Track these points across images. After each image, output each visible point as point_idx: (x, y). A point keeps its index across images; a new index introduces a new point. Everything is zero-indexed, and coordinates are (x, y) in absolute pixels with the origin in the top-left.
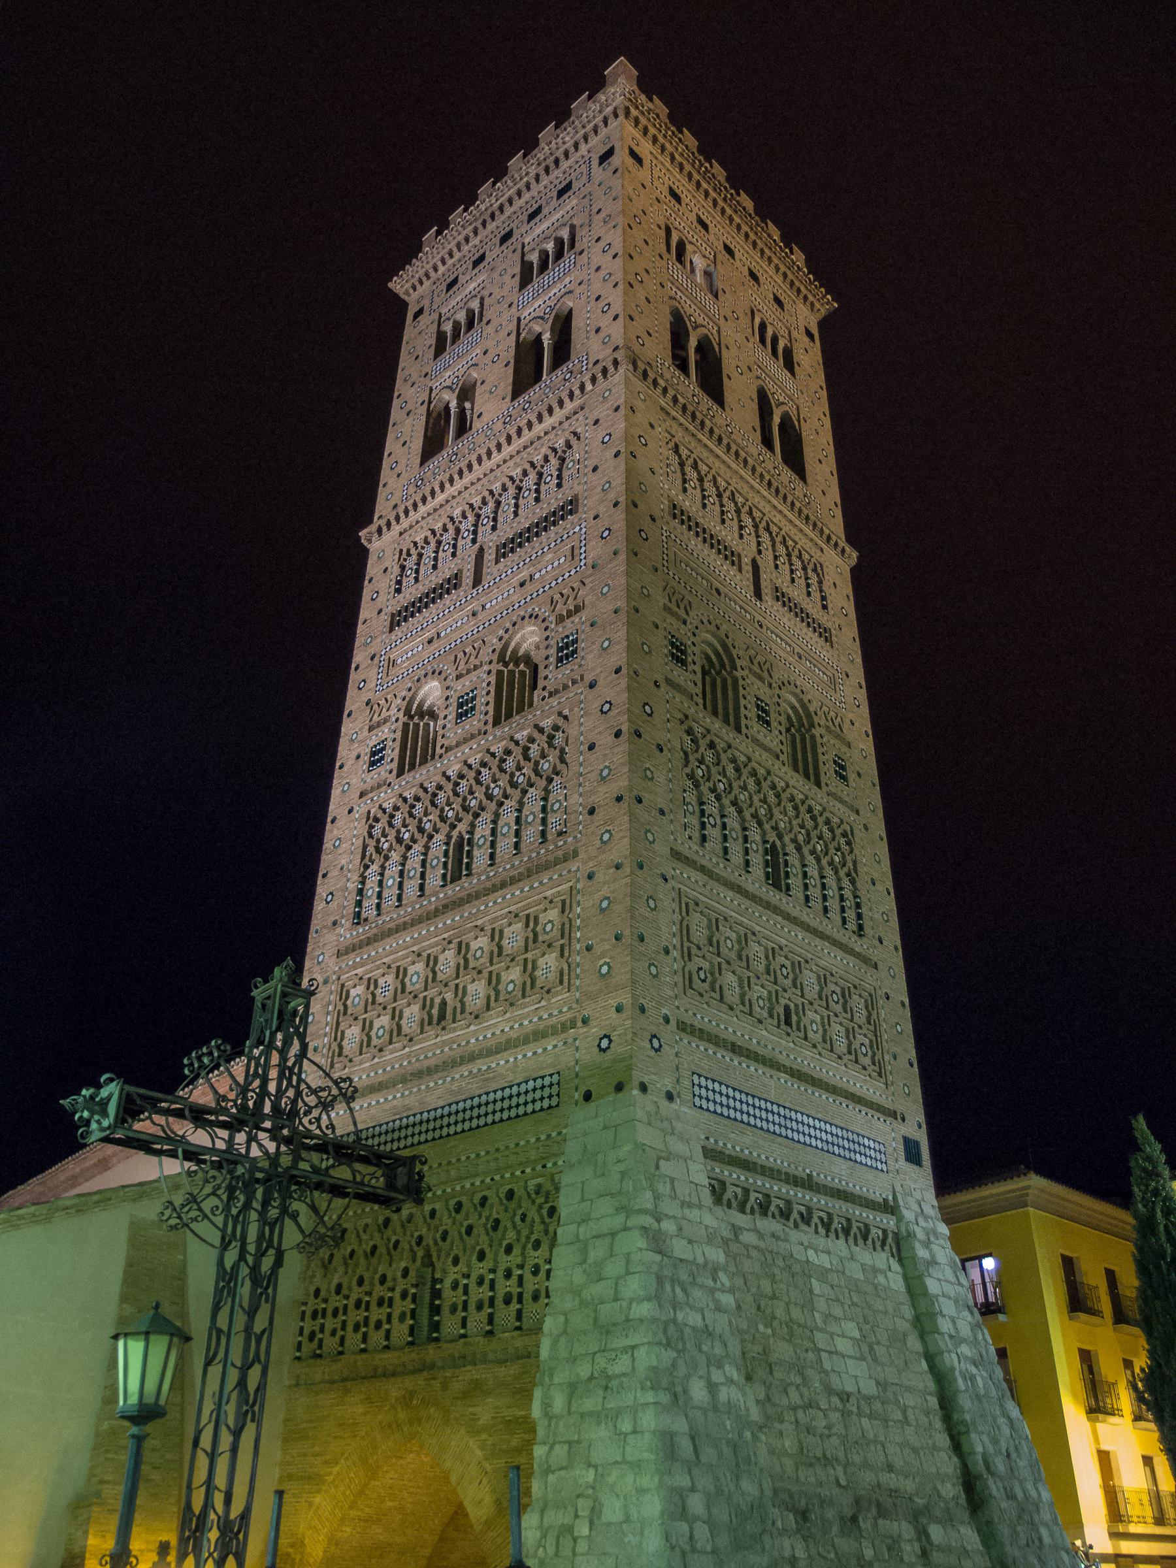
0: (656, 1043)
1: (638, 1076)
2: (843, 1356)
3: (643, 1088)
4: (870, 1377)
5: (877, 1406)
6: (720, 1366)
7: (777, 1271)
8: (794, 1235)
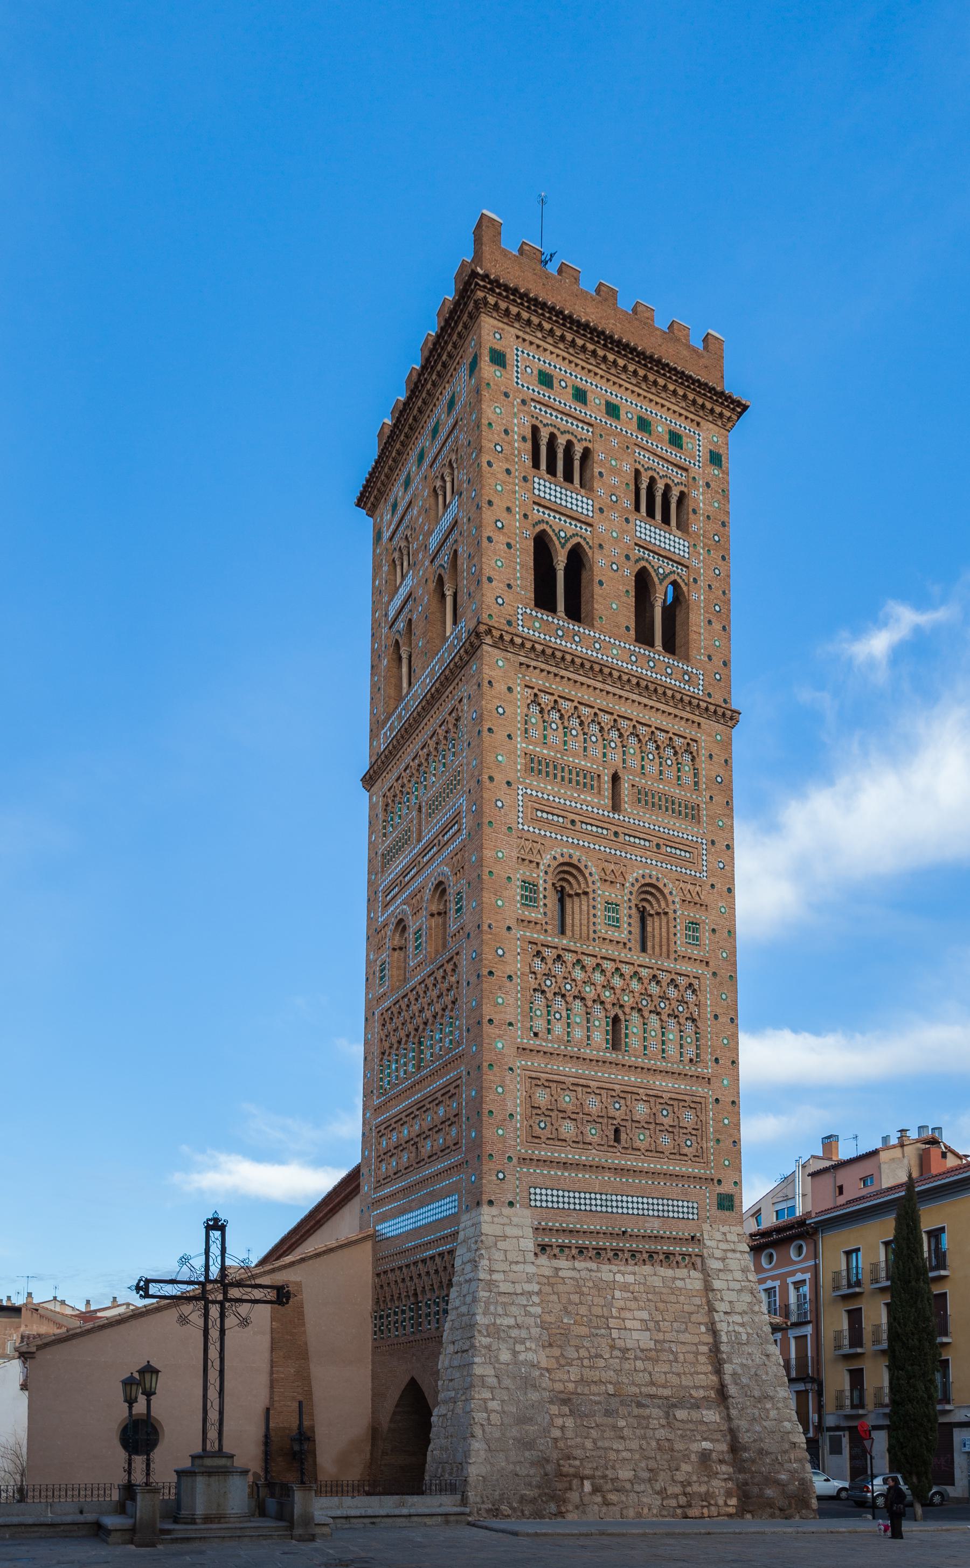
0: (501, 1175)
1: (485, 1198)
2: (630, 1330)
3: (491, 1203)
6: (523, 1342)
7: (584, 1289)
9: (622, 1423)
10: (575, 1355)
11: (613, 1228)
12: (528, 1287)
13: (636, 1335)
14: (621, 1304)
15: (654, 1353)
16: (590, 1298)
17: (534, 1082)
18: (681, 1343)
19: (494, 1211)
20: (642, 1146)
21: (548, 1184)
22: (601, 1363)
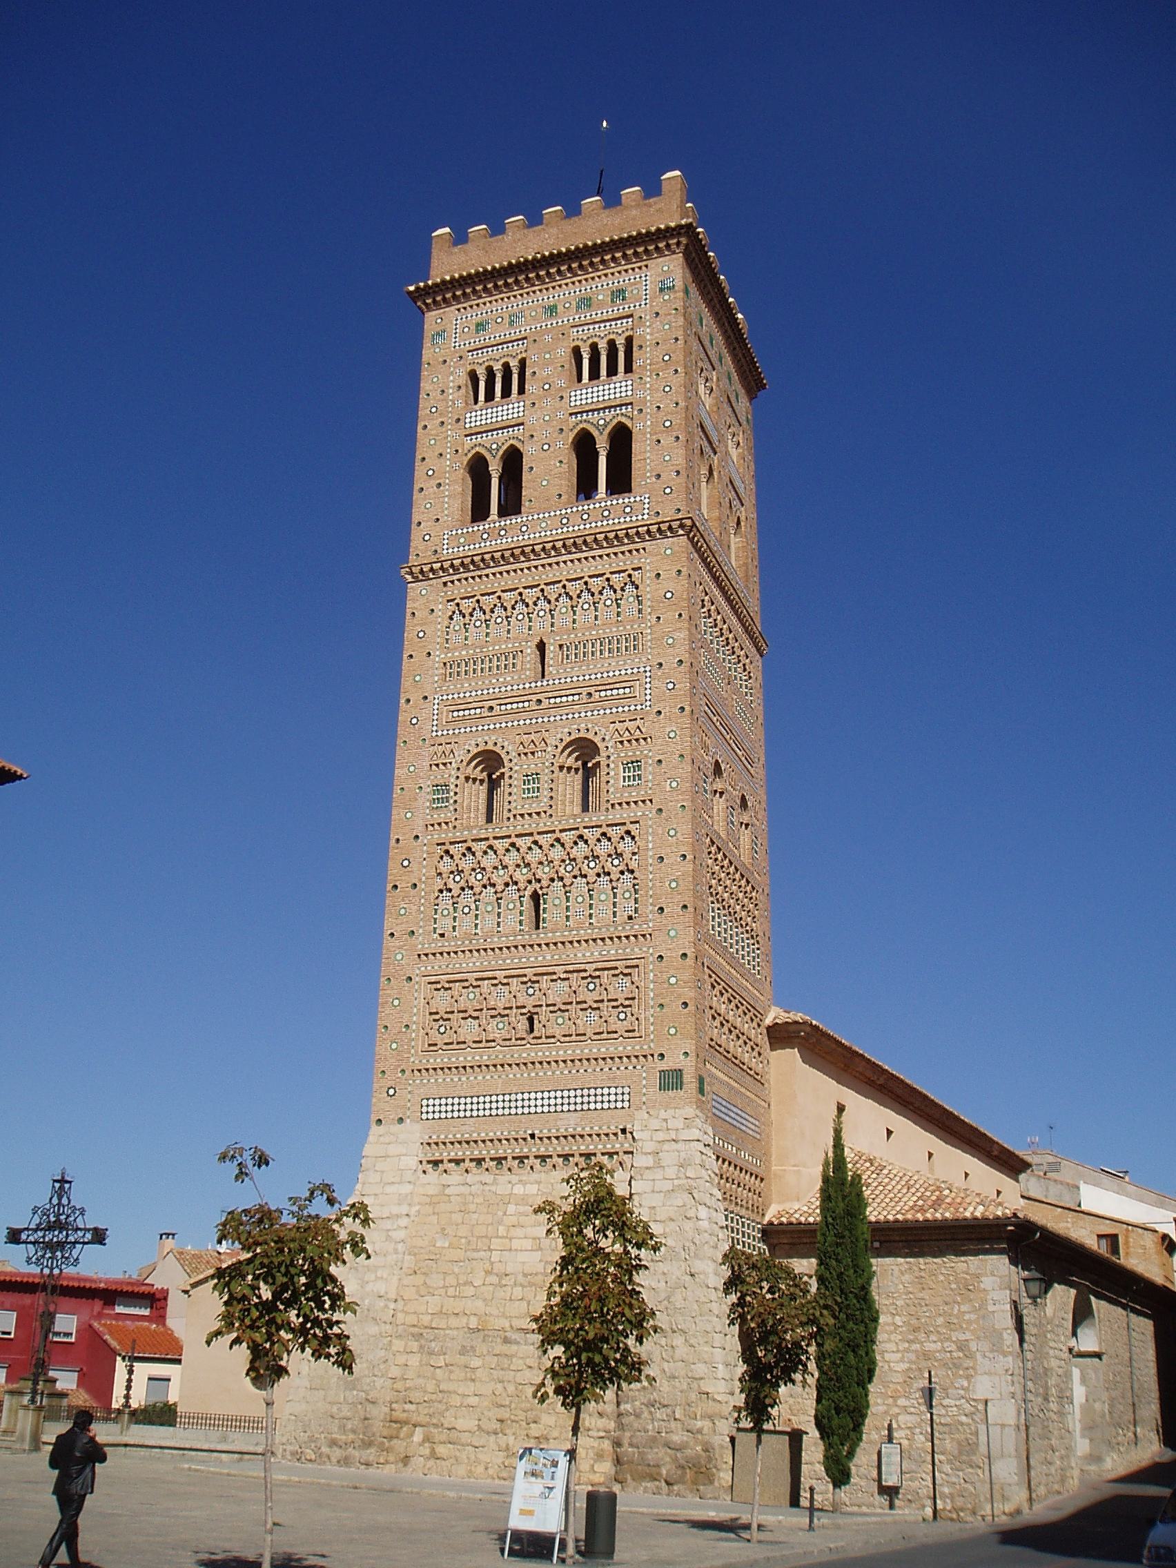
9: (476, 1362)
10: (441, 1283)
11: (517, 1132)
12: (396, 1210)
13: (522, 1257)
14: (513, 1220)
16: (475, 1216)
17: (435, 986)
19: (381, 1129)
20: (558, 1032)
21: (443, 1093)
22: (470, 1291)
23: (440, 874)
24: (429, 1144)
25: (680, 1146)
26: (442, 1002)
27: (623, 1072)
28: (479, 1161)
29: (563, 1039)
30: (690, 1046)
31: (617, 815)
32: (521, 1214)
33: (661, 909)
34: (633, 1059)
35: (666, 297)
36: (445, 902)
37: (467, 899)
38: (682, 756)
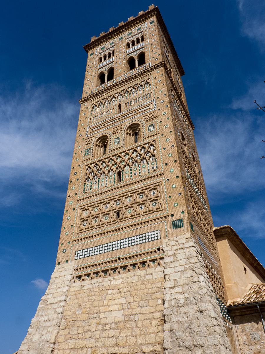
4: (123, 315)
5: (121, 324)
8: (108, 278)
10: (76, 332)
11: (113, 258)
13: (114, 314)
14: (110, 297)
15: (122, 323)
16: (94, 297)
18: (142, 314)
19: (60, 266)
22: (89, 335)
23: (86, 174)
24: (77, 269)
25: (186, 250)
26: (85, 214)
27: (156, 225)
28: (97, 273)
29: (131, 218)
30: (184, 209)
31: (147, 141)
32: (114, 294)
33: (166, 164)
34: (160, 219)
35: (152, 24)
36: (88, 182)
37: (96, 179)
38: (168, 118)
